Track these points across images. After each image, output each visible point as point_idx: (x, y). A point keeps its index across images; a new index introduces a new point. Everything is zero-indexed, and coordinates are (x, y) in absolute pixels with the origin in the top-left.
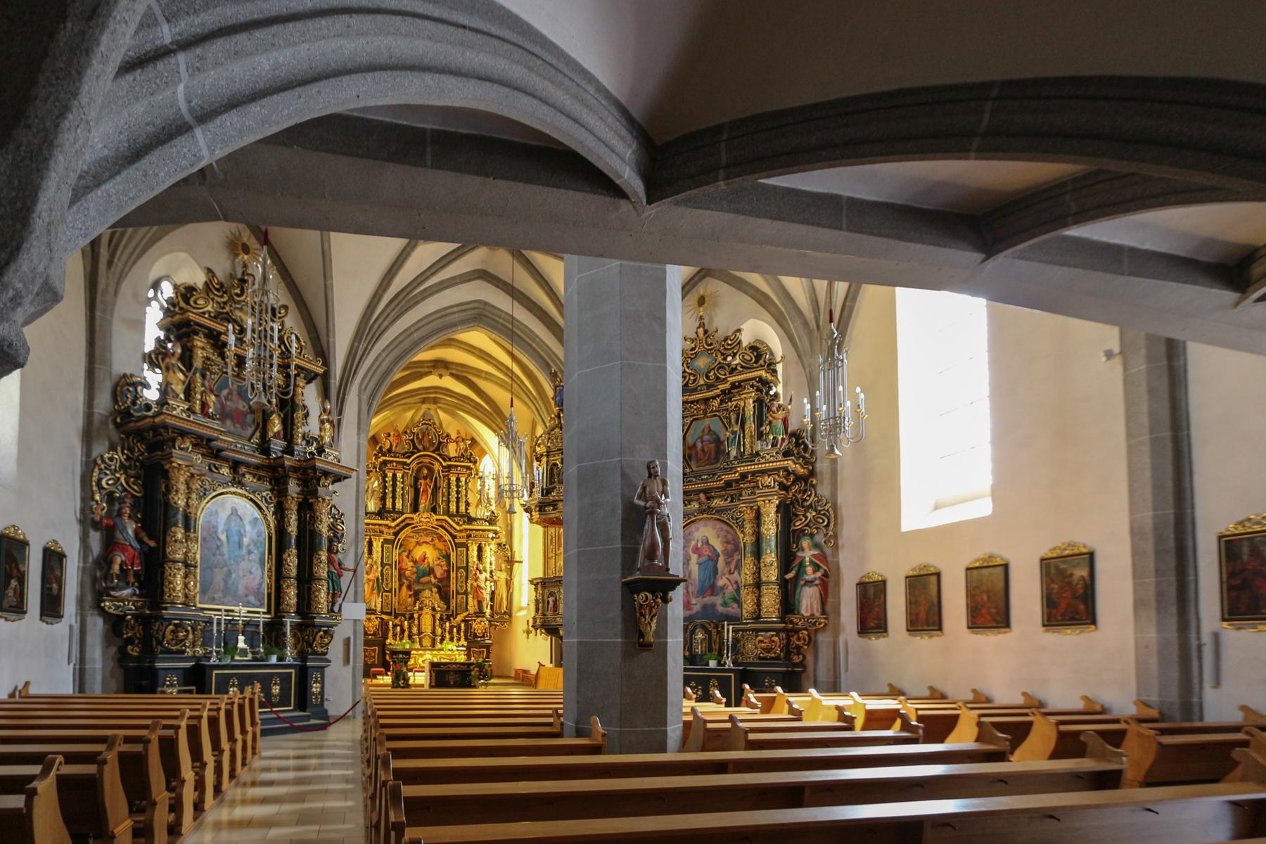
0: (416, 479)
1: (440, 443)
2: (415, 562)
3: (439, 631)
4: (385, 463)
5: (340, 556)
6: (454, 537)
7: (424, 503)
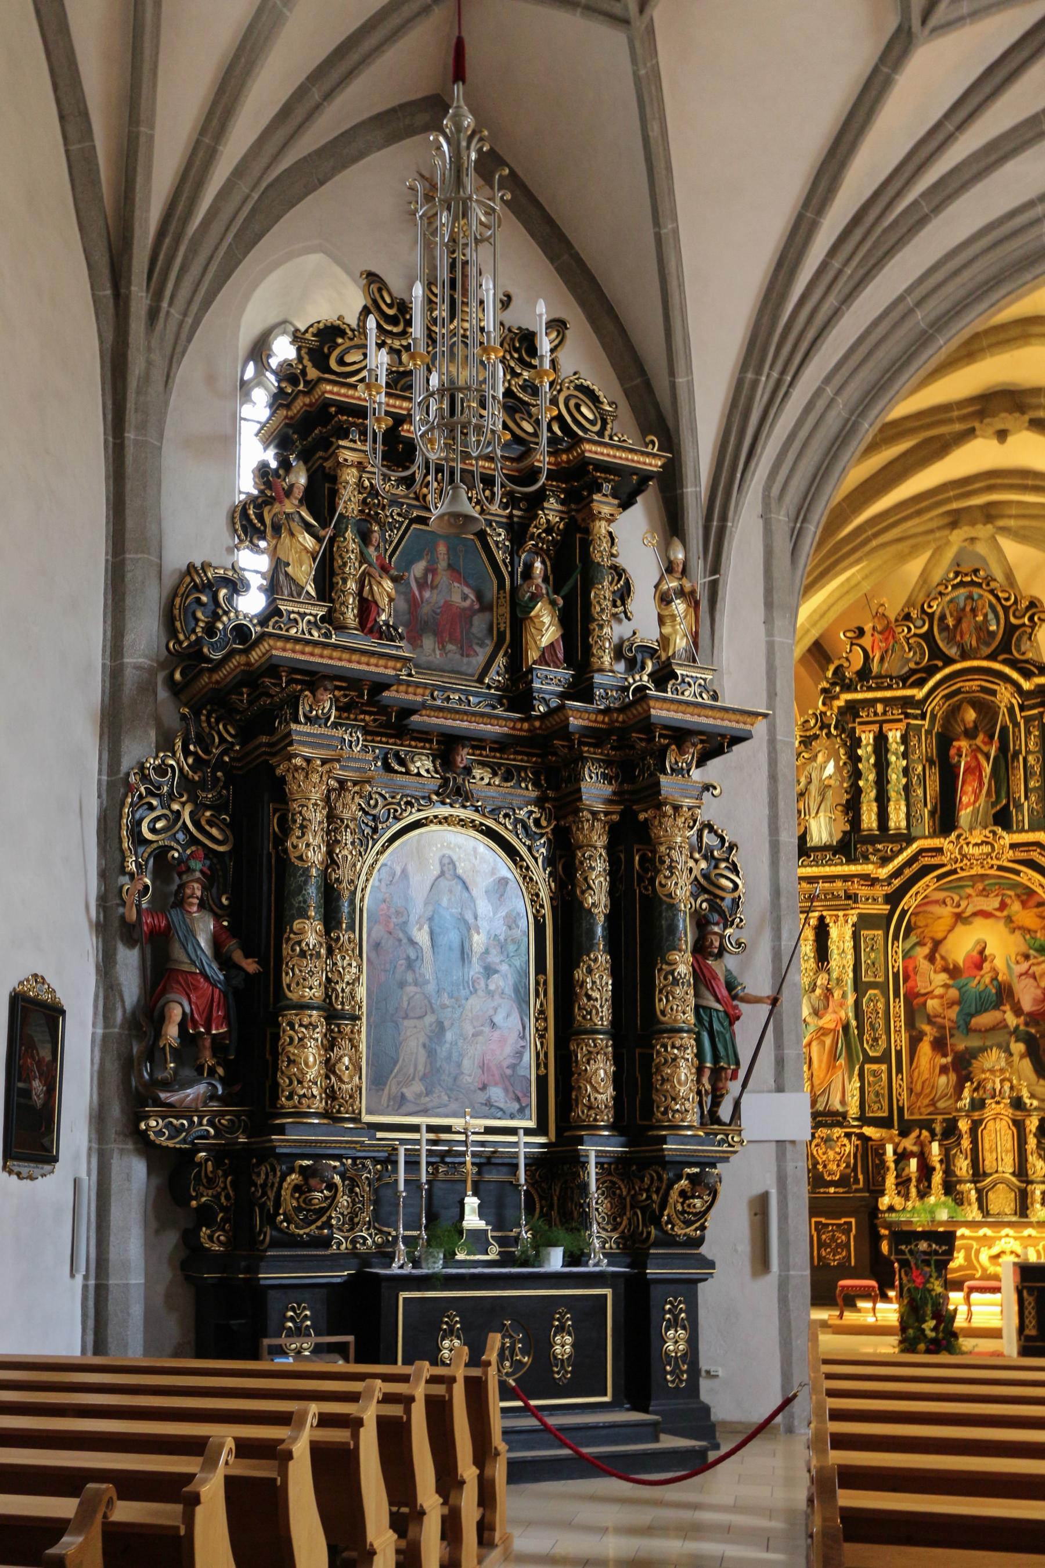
0: (945, 741)
4: (852, 709)
5: (730, 962)
7: (971, 803)
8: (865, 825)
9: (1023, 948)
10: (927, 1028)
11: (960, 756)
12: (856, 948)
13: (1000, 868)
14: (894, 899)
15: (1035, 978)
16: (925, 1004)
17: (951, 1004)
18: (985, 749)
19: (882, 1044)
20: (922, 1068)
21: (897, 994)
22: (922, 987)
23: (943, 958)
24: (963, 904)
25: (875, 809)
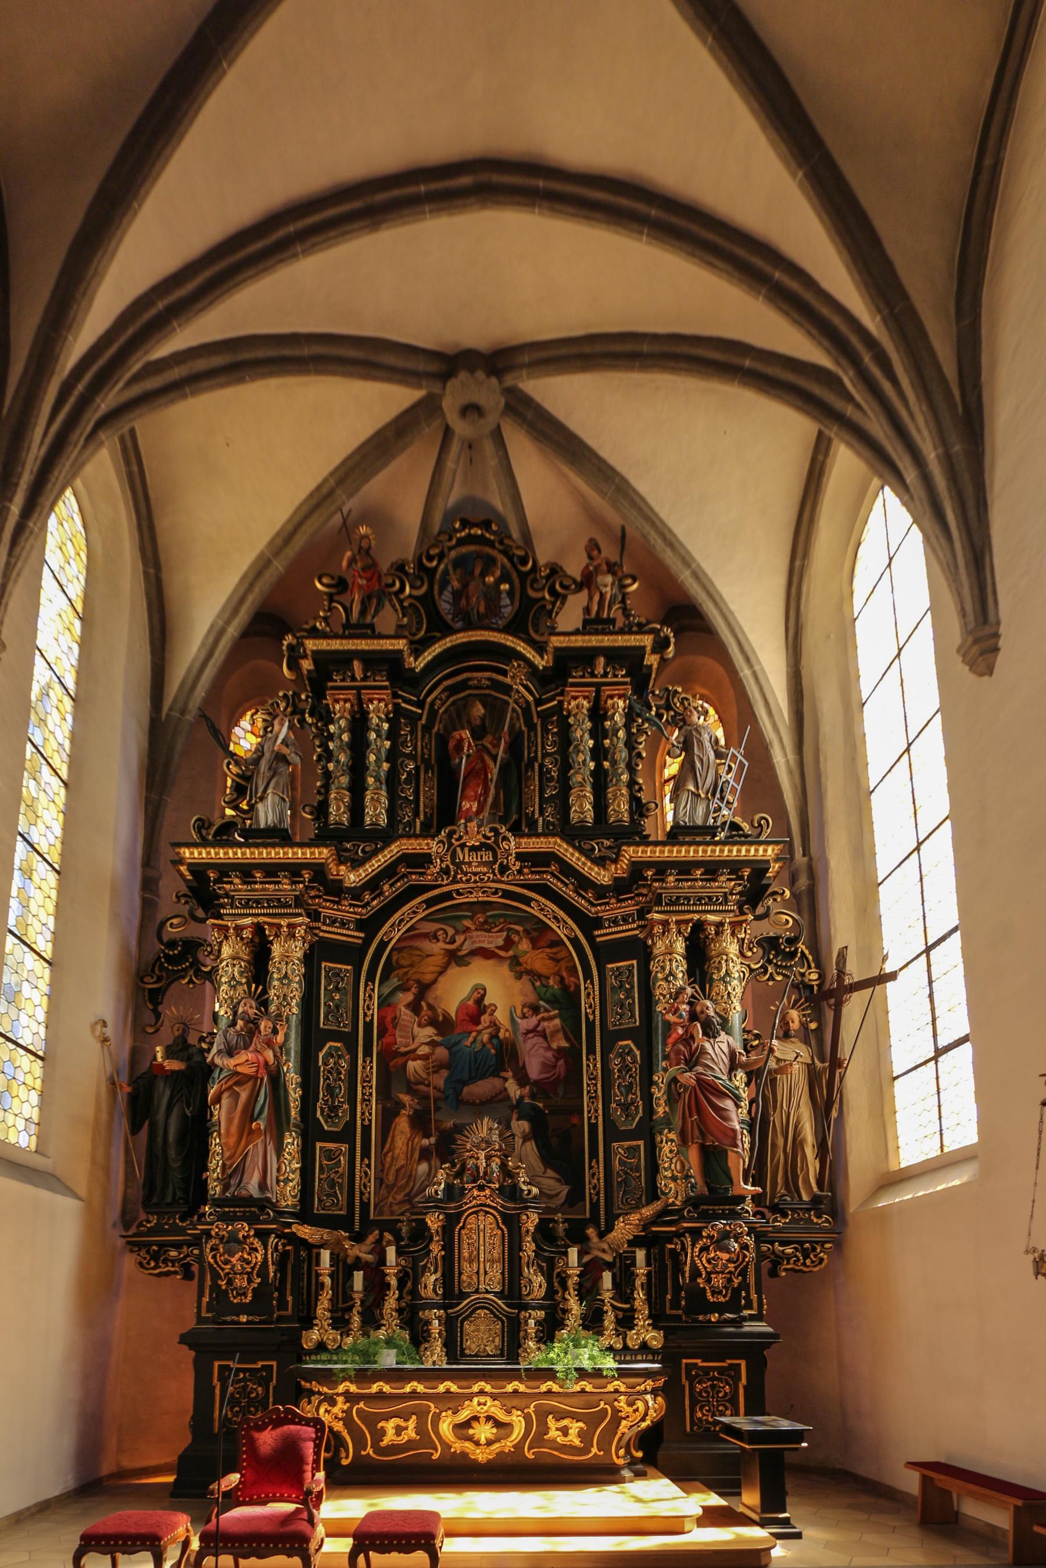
3: (536, 1283)
6: (589, 924)
9: (532, 998)
10: (406, 1099)
13: (507, 894)
14: (370, 926)
15: (545, 1037)
20: (397, 1151)
21: (368, 1052)
22: (401, 1043)
23: (431, 1007)
24: (459, 939)
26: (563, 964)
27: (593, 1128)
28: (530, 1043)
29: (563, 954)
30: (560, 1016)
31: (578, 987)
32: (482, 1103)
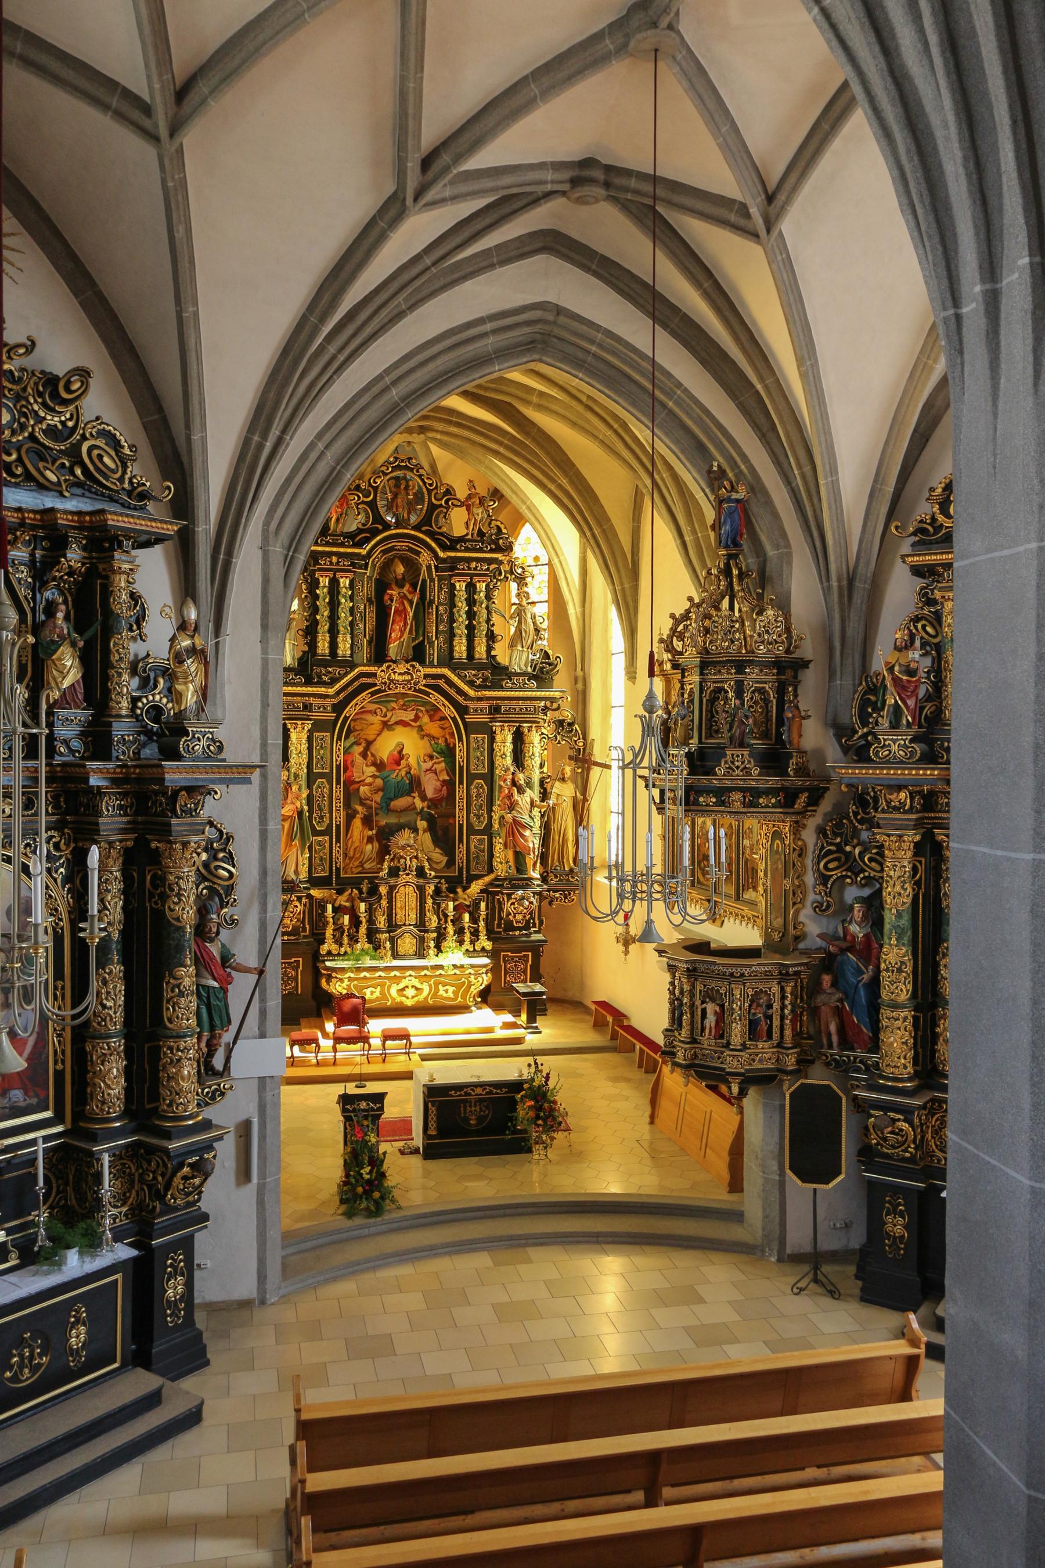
1: (432, 508)
2: (380, 766)
8: (319, 651)
9: (429, 751)
10: (359, 808)
11: (392, 601)
12: (310, 749)
14: (339, 708)
16: (358, 790)
17: (377, 791)
18: (410, 596)
19: (327, 820)
21: (338, 782)
22: (357, 776)
23: (373, 755)
24: (389, 714)
25: (328, 639)
26: (447, 731)
27: (461, 826)
28: (428, 776)
29: (447, 725)
30: (445, 761)
31: (455, 745)
32: (401, 811)
